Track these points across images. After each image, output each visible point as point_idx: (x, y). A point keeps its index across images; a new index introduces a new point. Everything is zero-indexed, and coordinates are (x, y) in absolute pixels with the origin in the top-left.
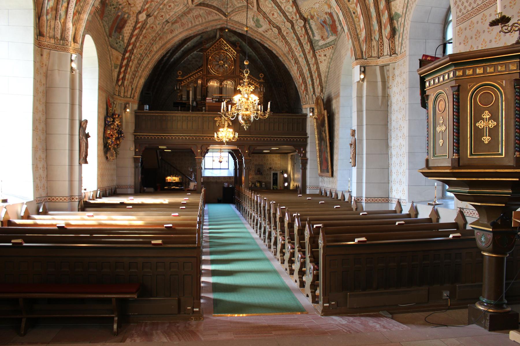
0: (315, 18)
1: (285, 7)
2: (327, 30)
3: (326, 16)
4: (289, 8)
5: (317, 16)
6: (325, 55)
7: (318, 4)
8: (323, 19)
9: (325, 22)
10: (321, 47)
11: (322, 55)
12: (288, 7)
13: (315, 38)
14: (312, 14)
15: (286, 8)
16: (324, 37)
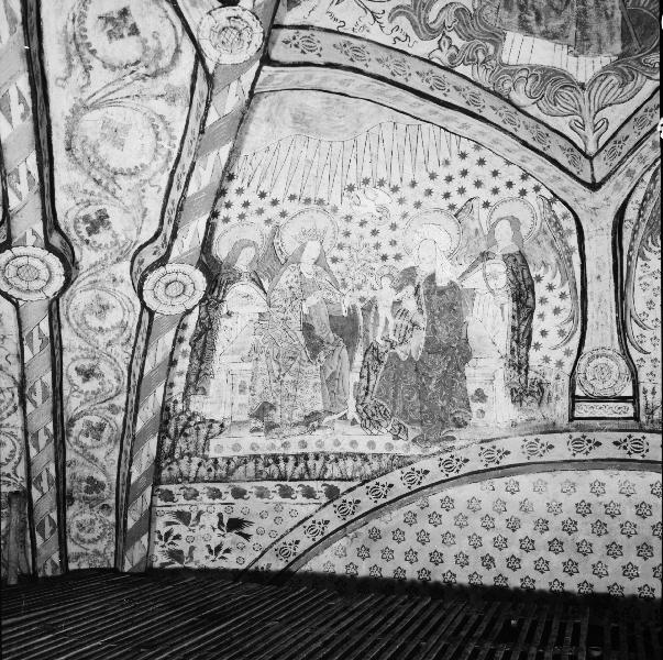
0: (287, 278)
1: (81, 108)
2: (332, 381)
3: (386, 296)
4: (116, 135)
5: (307, 267)
6: (236, 525)
7: (383, 196)
8: (346, 302)
9: (347, 329)
10: (223, 473)
11: (210, 520)
12: (115, 115)
13: (199, 405)
14: (289, 243)
15: (91, 123)
16: (276, 417)
